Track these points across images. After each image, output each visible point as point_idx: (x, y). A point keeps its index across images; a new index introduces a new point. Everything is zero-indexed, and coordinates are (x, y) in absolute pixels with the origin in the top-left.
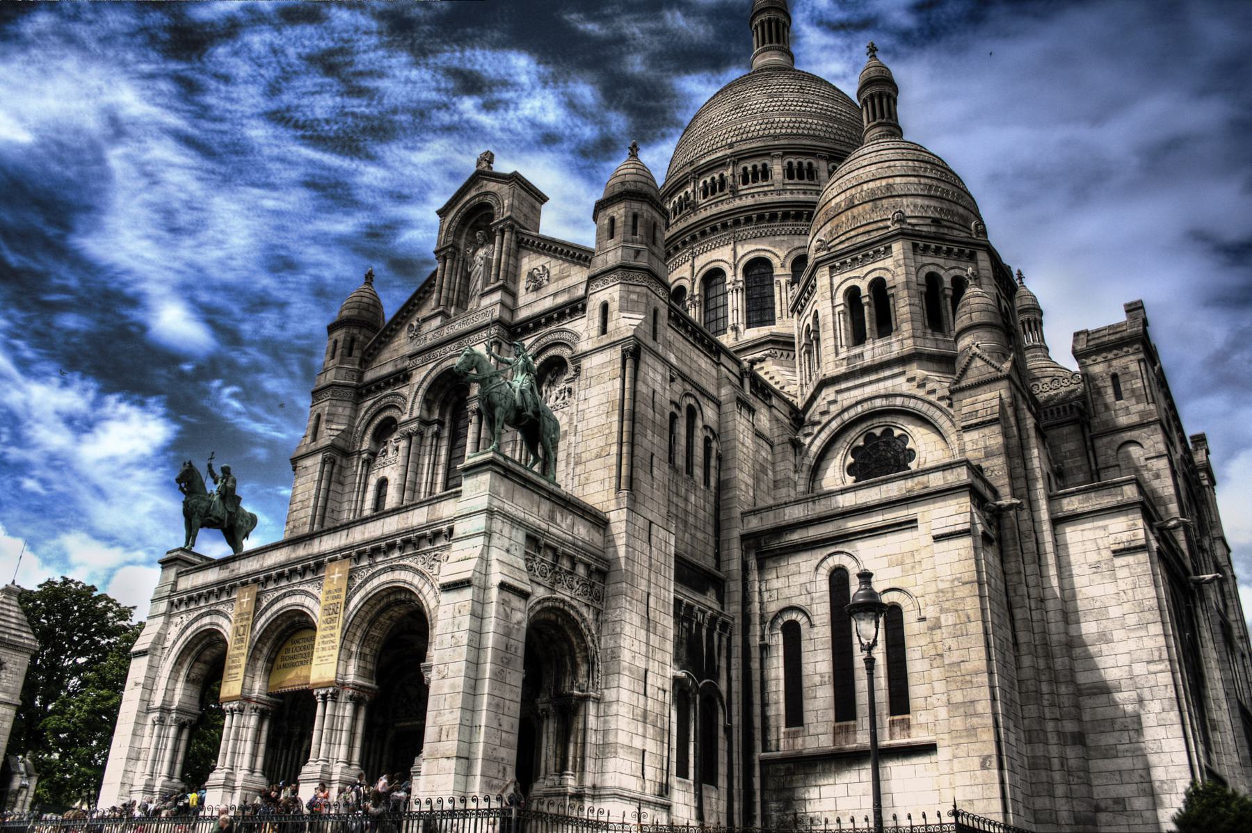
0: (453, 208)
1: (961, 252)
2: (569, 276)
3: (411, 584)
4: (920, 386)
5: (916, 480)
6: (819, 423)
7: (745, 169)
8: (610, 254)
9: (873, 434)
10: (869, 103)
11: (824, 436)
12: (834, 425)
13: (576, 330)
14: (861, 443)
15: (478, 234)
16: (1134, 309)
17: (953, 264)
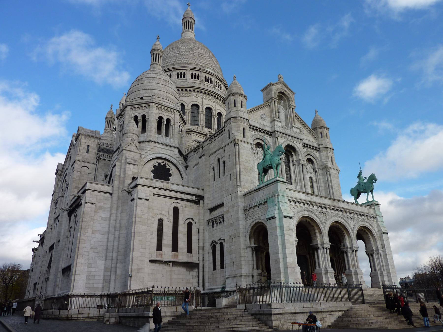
0: (275, 86)
3: (369, 227)
7: (217, 81)
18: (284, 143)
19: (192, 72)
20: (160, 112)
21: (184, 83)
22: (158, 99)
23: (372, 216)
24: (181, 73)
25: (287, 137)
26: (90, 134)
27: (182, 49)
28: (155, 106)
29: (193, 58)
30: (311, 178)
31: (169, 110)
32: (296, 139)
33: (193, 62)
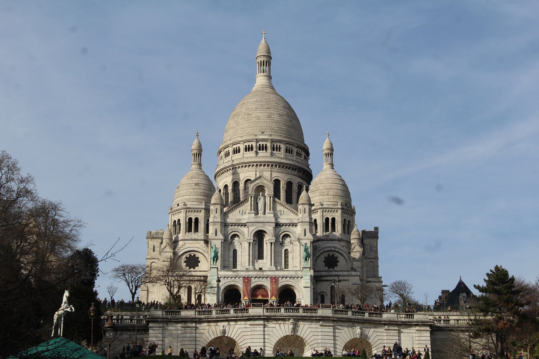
1: (350, 214)
2: (289, 215)
4: (342, 247)
5: (350, 272)
6: (318, 249)
7: (274, 145)
8: (306, 218)
9: (330, 255)
10: (327, 155)
11: (319, 253)
12: (322, 251)
13: (294, 230)
14: (327, 256)
15: (261, 193)
16: (376, 229)
17: (349, 216)
18: (254, 230)
19: (245, 145)
20: (189, 214)
21: (237, 160)
22: (189, 203)
23: (297, 277)
24: (236, 148)
25: (258, 224)
26: (154, 236)
27: (240, 117)
28: (185, 211)
29: (248, 127)
30: (286, 250)
31: (196, 210)
32: (267, 224)
33: (248, 131)
